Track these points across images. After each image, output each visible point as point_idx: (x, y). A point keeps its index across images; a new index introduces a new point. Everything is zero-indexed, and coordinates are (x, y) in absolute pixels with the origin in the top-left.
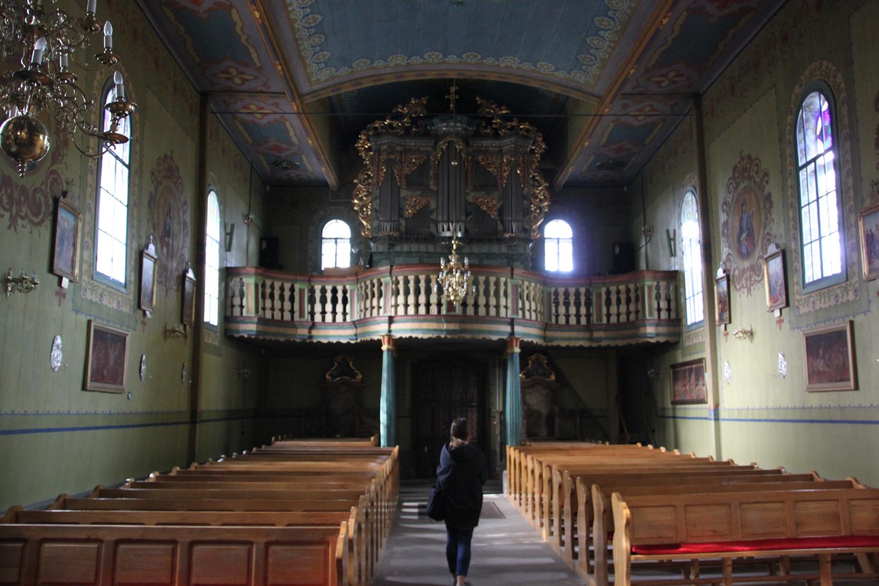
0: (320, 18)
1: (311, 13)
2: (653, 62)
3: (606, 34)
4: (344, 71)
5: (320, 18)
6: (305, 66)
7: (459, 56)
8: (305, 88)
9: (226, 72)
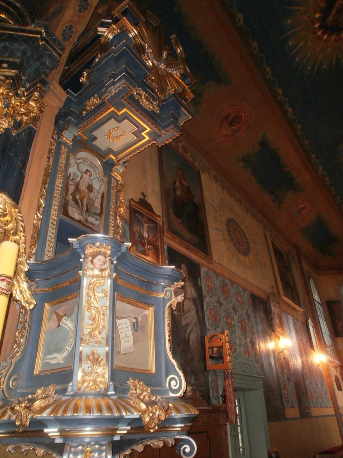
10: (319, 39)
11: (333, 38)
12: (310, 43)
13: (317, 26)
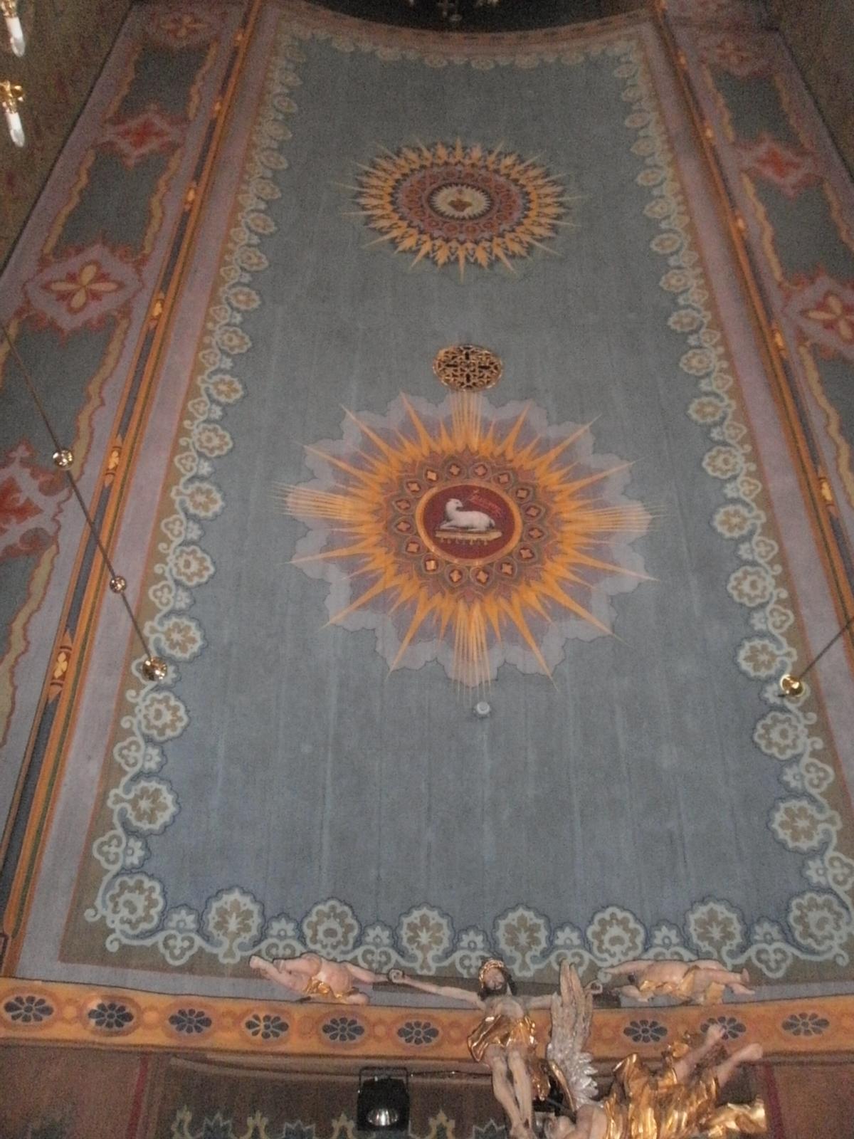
0: (627, 123)
1: (637, 130)
2: (213, 51)
3: (278, 90)
4: (596, 50)
5: (627, 123)
6: (646, 61)
7: (450, 63)
8: (647, 30)
9: (742, 59)
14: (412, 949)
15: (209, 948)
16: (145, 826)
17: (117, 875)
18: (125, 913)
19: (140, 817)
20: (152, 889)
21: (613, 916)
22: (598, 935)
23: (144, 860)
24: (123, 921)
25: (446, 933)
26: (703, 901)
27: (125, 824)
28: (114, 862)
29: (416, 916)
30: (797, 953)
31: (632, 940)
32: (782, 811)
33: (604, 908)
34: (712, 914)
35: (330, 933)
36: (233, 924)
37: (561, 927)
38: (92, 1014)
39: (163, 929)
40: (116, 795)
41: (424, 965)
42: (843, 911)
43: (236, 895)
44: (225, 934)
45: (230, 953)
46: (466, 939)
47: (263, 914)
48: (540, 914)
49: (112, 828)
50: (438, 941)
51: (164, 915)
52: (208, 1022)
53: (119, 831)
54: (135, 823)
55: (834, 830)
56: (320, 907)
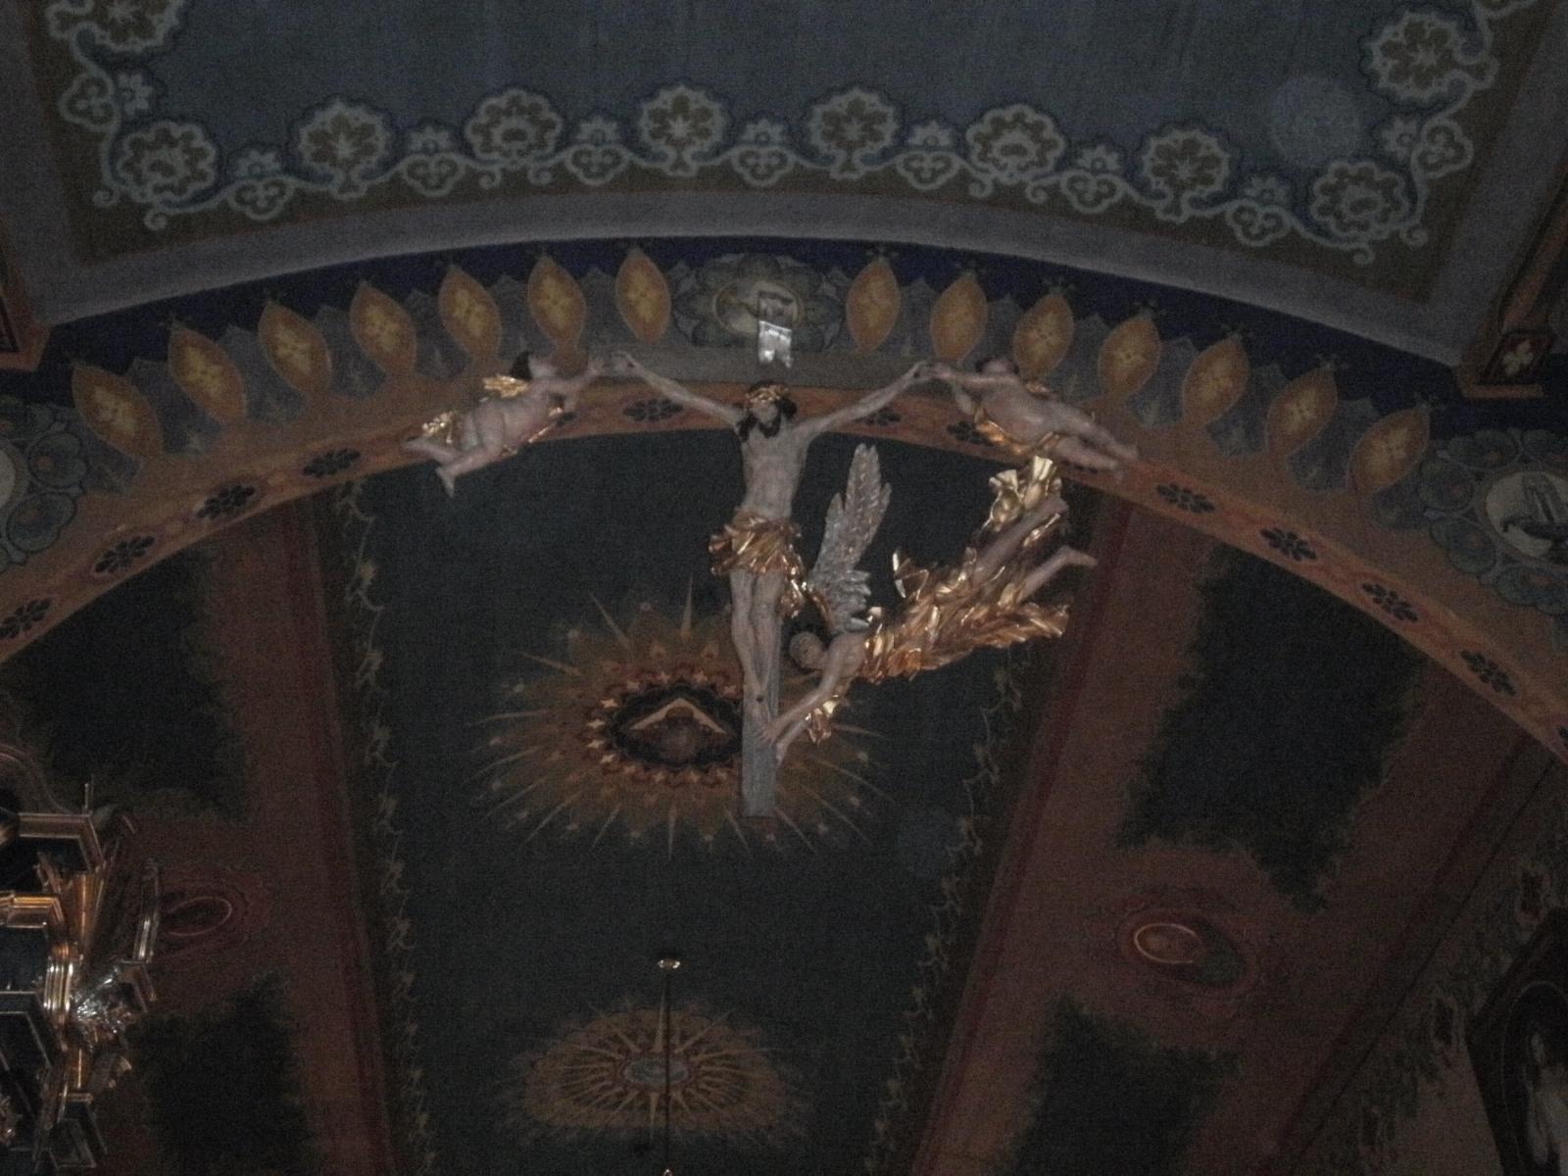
10: (590, 757)
11: (629, 769)
12: (556, 756)
13: (596, 724)
14: (661, 146)
15: (311, 187)
16: (137, 45)
17: (120, 136)
18: (158, 178)
19: (120, 34)
20: (188, 137)
21: (1019, 118)
22: (985, 141)
23: (156, 100)
24: (158, 190)
25: (718, 123)
26: (1182, 125)
27: (99, 55)
28: (106, 119)
29: (666, 99)
30: (1300, 228)
31: (1041, 154)
32: (1401, 27)
33: (1004, 105)
34: (1191, 147)
35: (514, 135)
36: (344, 149)
37: (924, 122)
38: (201, 514)
39: (229, 183)
40: (59, 15)
41: (679, 164)
42: (1406, 204)
43: (338, 108)
44: (334, 164)
45: (348, 186)
46: (751, 131)
47: (391, 124)
48: (888, 98)
49: (77, 69)
50: (705, 133)
51: (223, 165)
52: (356, 455)
53: (94, 70)
54: (117, 48)
55: (1472, 86)
56: (493, 101)
